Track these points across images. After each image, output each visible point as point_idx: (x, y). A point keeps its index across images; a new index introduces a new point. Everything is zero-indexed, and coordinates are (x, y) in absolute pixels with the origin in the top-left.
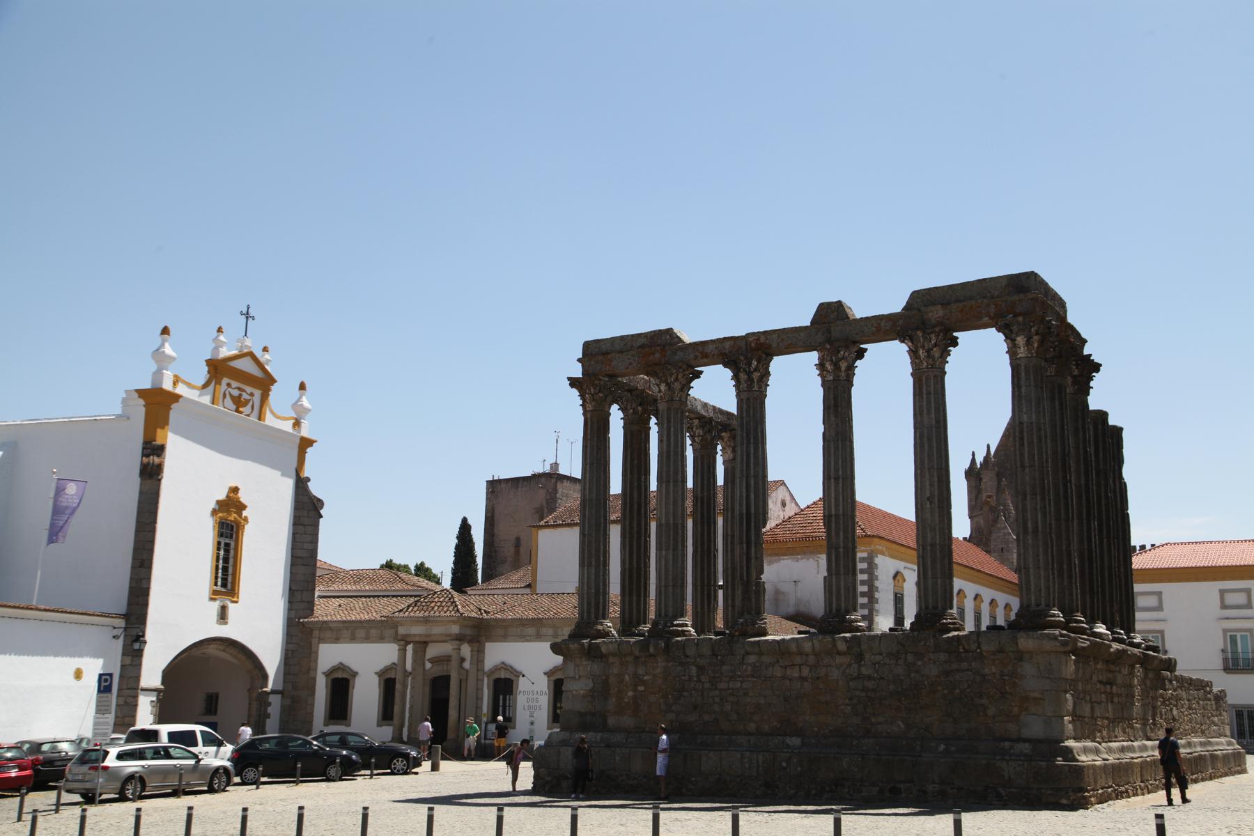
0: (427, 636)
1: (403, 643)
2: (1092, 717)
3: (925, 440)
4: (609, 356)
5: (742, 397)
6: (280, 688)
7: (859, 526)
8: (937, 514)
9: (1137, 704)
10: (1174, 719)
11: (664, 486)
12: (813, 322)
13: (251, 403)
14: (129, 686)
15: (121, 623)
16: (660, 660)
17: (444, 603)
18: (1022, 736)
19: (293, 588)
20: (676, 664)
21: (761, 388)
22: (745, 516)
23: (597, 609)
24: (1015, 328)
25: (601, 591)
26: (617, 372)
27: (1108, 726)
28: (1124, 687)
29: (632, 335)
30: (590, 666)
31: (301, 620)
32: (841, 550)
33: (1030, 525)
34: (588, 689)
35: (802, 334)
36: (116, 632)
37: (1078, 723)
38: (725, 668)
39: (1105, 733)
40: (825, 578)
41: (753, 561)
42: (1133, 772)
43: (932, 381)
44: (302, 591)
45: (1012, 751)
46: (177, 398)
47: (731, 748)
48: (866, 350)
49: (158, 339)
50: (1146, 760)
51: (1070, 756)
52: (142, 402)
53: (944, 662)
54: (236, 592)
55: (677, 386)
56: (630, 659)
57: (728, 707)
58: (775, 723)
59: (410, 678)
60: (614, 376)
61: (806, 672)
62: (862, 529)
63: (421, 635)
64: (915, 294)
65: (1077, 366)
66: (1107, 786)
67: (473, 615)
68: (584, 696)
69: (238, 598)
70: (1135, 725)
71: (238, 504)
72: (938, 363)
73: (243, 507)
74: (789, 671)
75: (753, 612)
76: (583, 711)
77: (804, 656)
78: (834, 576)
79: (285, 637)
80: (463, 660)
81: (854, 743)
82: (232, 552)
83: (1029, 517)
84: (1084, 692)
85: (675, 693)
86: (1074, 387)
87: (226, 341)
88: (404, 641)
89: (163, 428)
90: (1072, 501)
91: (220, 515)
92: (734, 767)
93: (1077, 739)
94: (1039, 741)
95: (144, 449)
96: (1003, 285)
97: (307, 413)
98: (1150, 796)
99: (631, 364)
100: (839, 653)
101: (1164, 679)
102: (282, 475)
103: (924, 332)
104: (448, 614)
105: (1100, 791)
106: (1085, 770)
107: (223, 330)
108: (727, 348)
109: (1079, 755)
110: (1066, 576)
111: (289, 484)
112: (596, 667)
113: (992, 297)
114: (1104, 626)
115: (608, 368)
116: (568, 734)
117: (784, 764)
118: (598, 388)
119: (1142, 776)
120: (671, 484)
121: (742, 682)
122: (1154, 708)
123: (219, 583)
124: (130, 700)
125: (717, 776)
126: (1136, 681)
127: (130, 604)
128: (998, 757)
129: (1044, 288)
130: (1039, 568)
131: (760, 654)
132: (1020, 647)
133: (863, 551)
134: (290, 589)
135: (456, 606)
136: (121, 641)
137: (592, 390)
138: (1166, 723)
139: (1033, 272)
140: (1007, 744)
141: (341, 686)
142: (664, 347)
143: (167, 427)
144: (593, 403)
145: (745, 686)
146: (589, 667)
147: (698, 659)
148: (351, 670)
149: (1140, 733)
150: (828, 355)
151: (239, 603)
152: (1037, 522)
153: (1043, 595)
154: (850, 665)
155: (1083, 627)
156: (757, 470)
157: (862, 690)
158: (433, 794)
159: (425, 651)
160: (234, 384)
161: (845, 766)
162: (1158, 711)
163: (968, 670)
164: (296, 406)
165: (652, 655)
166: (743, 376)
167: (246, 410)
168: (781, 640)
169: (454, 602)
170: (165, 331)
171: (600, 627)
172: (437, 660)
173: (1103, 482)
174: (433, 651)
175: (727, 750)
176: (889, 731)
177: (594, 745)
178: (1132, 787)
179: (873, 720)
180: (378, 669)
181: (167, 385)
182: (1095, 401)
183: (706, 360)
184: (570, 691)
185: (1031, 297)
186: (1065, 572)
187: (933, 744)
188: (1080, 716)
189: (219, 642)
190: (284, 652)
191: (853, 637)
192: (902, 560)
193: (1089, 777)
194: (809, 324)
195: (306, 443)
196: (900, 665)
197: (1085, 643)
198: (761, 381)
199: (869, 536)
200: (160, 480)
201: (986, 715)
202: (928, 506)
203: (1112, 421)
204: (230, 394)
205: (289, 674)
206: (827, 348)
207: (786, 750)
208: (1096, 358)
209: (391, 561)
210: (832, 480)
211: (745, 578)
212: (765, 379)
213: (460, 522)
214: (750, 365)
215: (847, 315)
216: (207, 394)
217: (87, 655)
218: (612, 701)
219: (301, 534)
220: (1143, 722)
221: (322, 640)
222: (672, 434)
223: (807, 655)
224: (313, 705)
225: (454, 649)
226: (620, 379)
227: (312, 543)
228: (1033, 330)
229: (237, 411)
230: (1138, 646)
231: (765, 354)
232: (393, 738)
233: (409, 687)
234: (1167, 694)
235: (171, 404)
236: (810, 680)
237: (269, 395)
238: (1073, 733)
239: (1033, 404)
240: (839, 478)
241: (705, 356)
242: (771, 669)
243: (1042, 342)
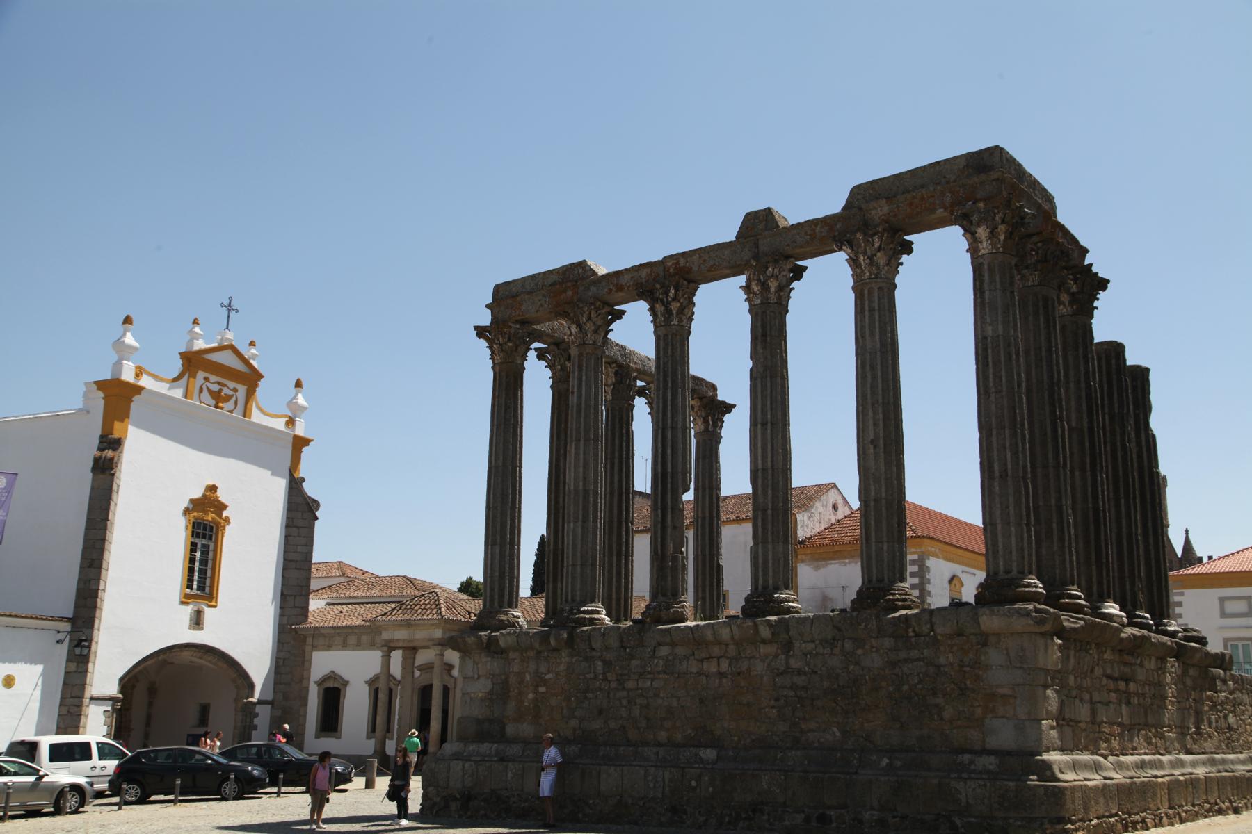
0: (410, 641)
1: (386, 649)
2: (1093, 722)
3: (868, 368)
4: (519, 299)
5: (659, 333)
6: (270, 697)
7: (910, 527)
8: (882, 461)
9: (1170, 707)
10: (1230, 728)
11: (573, 446)
12: (737, 237)
13: (234, 399)
14: (73, 695)
15: (67, 627)
16: (563, 654)
17: (429, 606)
18: (988, 746)
19: (285, 593)
20: (581, 659)
21: (682, 321)
22: (660, 475)
23: (501, 596)
24: (975, 218)
25: (507, 574)
26: (527, 316)
27: (1121, 735)
28: (1149, 685)
29: (544, 273)
30: (489, 664)
31: (293, 627)
32: (769, 512)
33: (996, 467)
34: (487, 690)
35: (726, 252)
36: (61, 636)
37: (1068, 730)
38: (634, 663)
39: (1115, 743)
40: (751, 547)
41: (669, 531)
42: (1154, 794)
43: (876, 295)
44: (295, 596)
45: (973, 767)
46: (138, 390)
47: (635, 763)
48: (806, 268)
49: (120, 328)
50: (1178, 780)
51: (1048, 773)
52: (101, 394)
53: (889, 650)
54: (215, 596)
55: (590, 327)
56: (531, 654)
57: (636, 711)
58: (689, 731)
59: (399, 687)
60: (528, 322)
61: (725, 666)
62: (913, 530)
63: (404, 640)
64: (855, 190)
65: (1075, 280)
66: (1107, 814)
67: (460, 618)
68: (482, 700)
69: (216, 602)
70: (1166, 734)
71: (216, 503)
72: (883, 272)
73: (224, 507)
74: (705, 665)
75: (669, 594)
76: (480, 717)
77: (723, 646)
78: (760, 545)
79: (276, 644)
80: (449, 667)
81: (779, 757)
82: (211, 554)
83: (996, 457)
84: (1080, 688)
85: (579, 695)
86: (1072, 307)
87: (201, 332)
88: (389, 648)
89: (122, 421)
90: (1064, 442)
91: (195, 514)
92: (636, 786)
93: (1062, 750)
94: (1009, 753)
95: (101, 442)
96: (961, 167)
97: (303, 412)
98: (1181, 827)
99: (541, 306)
100: (764, 642)
101: (1213, 678)
102: (272, 474)
103: (865, 234)
104: (430, 617)
105: (1095, 822)
106: (1068, 793)
107: (199, 322)
108: (643, 277)
109: (1063, 773)
110: (1055, 538)
111: (279, 487)
112: (495, 664)
113: (948, 182)
114: (1117, 606)
115: (517, 313)
116: (462, 745)
117: (694, 783)
118: (507, 336)
119: (1169, 800)
120: (582, 443)
121: (652, 680)
122: (1199, 716)
123: (195, 586)
124: (74, 710)
125: (618, 798)
126: (1168, 679)
127: (77, 606)
128: (953, 775)
129: (1015, 169)
130: (1009, 523)
131: (673, 644)
132: (983, 627)
133: (914, 553)
134: (282, 594)
135: (440, 608)
136: (65, 646)
137: (501, 339)
138: (1218, 733)
139: (997, 146)
140: (967, 757)
141: (332, 696)
142: (576, 282)
143: (126, 420)
144: (501, 354)
145: (655, 684)
146: (488, 664)
147: (605, 653)
148: (342, 679)
149: (1176, 745)
150: (754, 274)
151: (218, 607)
152: (1005, 464)
153: (1014, 558)
154: (776, 656)
155: (1079, 604)
156: (675, 420)
157: (791, 688)
158: (298, 817)
159: (414, 658)
160: (213, 378)
161: (765, 787)
162: (1205, 718)
163: (919, 659)
164: (292, 404)
165: (556, 650)
166: (660, 308)
167: (229, 405)
168: (695, 626)
169: (439, 604)
170: (128, 320)
171: (503, 617)
172: (427, 668)
173: (1118, 429)
174: (423, 657)
175: (631, 765)
176: (822, 740)
177: (486, 759)
178: (1152, 814)
179: (803, 727)
180: (368, 678)
181: (128, 375)
182: (1103, 329)
183: (621, 294)
184: (468, 693)
185: (995, 176)
186: (1055, 532)
187: (874, 757)
188: (1071, 720)
189: (194, 649)
190: (274, 659)
191: (780, 621)
192: (959, 563)
193: (1073, 802)
194: (734, 239)
195: (300, 443)
196: (835, 655)
197: (1077, 623)
198: (682, 313)
199: (919, 537)
200: (113, 475)
201: (942, 719)
202: (872, 451)
203: (1132, 359)
204: (208, 389)
205: (281, 684)
206: (752, 265)
207: (697, 765)
208: (1100, 269)
209: (471, 578)
210: (759, 426)
211: (659, 551)
212: (686, 311)
213: (538, 540)
214: (667, 293)
215: (777, 223)
216: (178, 387)
217: (21, 661)
218: (512, 705)
219: (294, 536)
220: (1179, 730)
221: (315, 647)
222: (584, 383)
223: (727, 645)
224: (305, 716)
225: (436, 655)
226: (535, 327)
227: (306, 545)
228: (997, 218)
229: (216, 406)
230: (1173, 635)
231: (685, 280)
232: (375, 752)
233: (399, 697)
234: (1218, 697)
235: (132, 397)
236: (730, 676)
237: (255, 391)
238: (1059, 743)
239: (1000, 311)
240: (766, 424)
241: (620, 288)
242: (685, 663)
243: (1011, 233)
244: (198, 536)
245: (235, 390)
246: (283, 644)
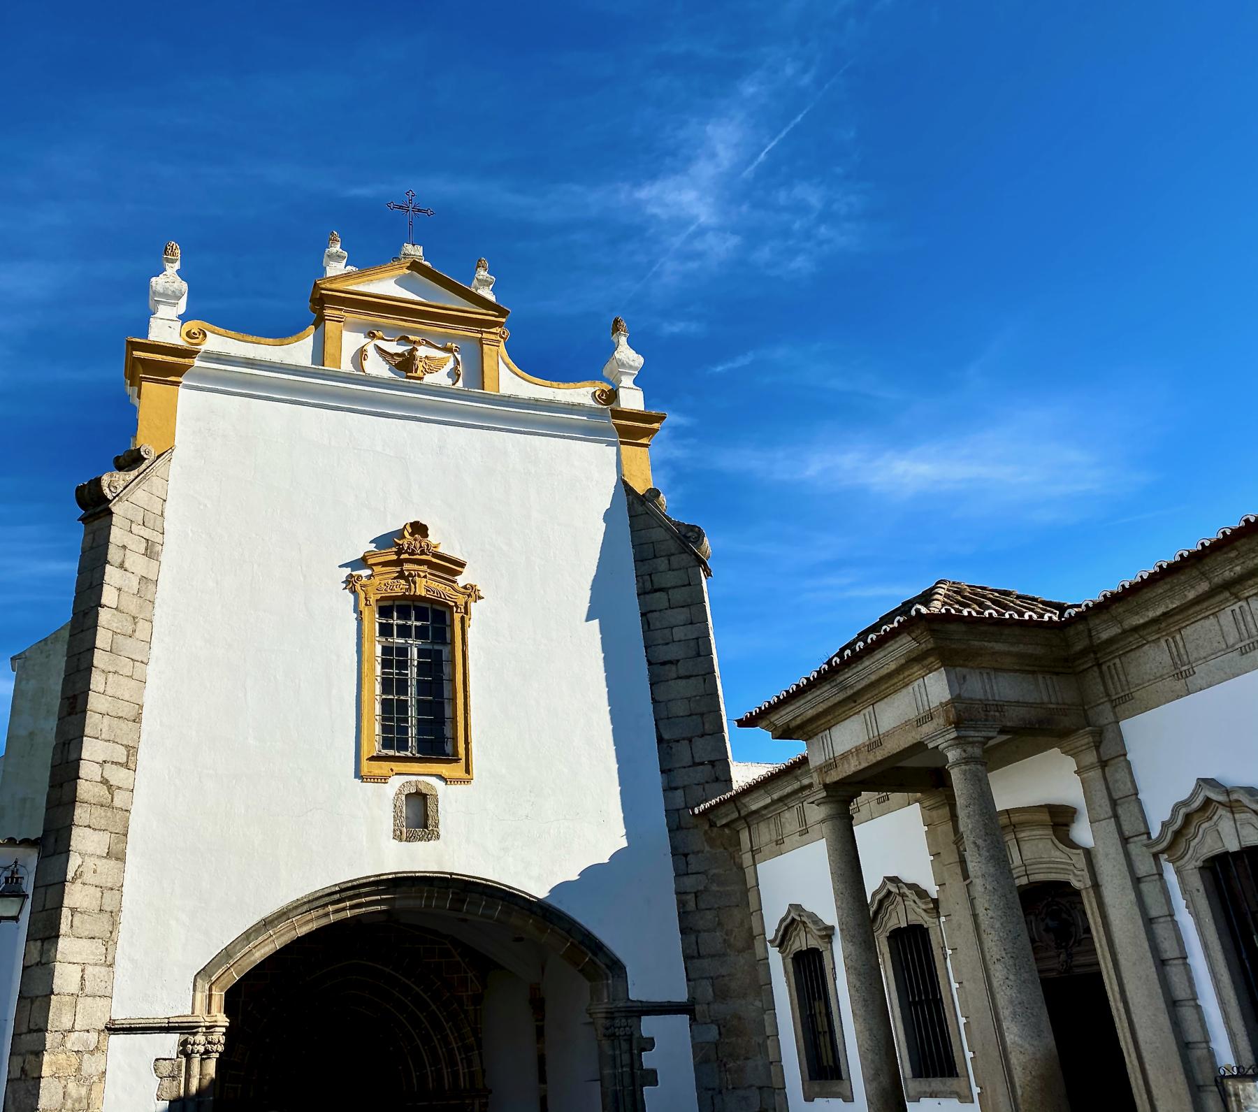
19: (666, 736)
31: (696, 811)
134: (660, 740)
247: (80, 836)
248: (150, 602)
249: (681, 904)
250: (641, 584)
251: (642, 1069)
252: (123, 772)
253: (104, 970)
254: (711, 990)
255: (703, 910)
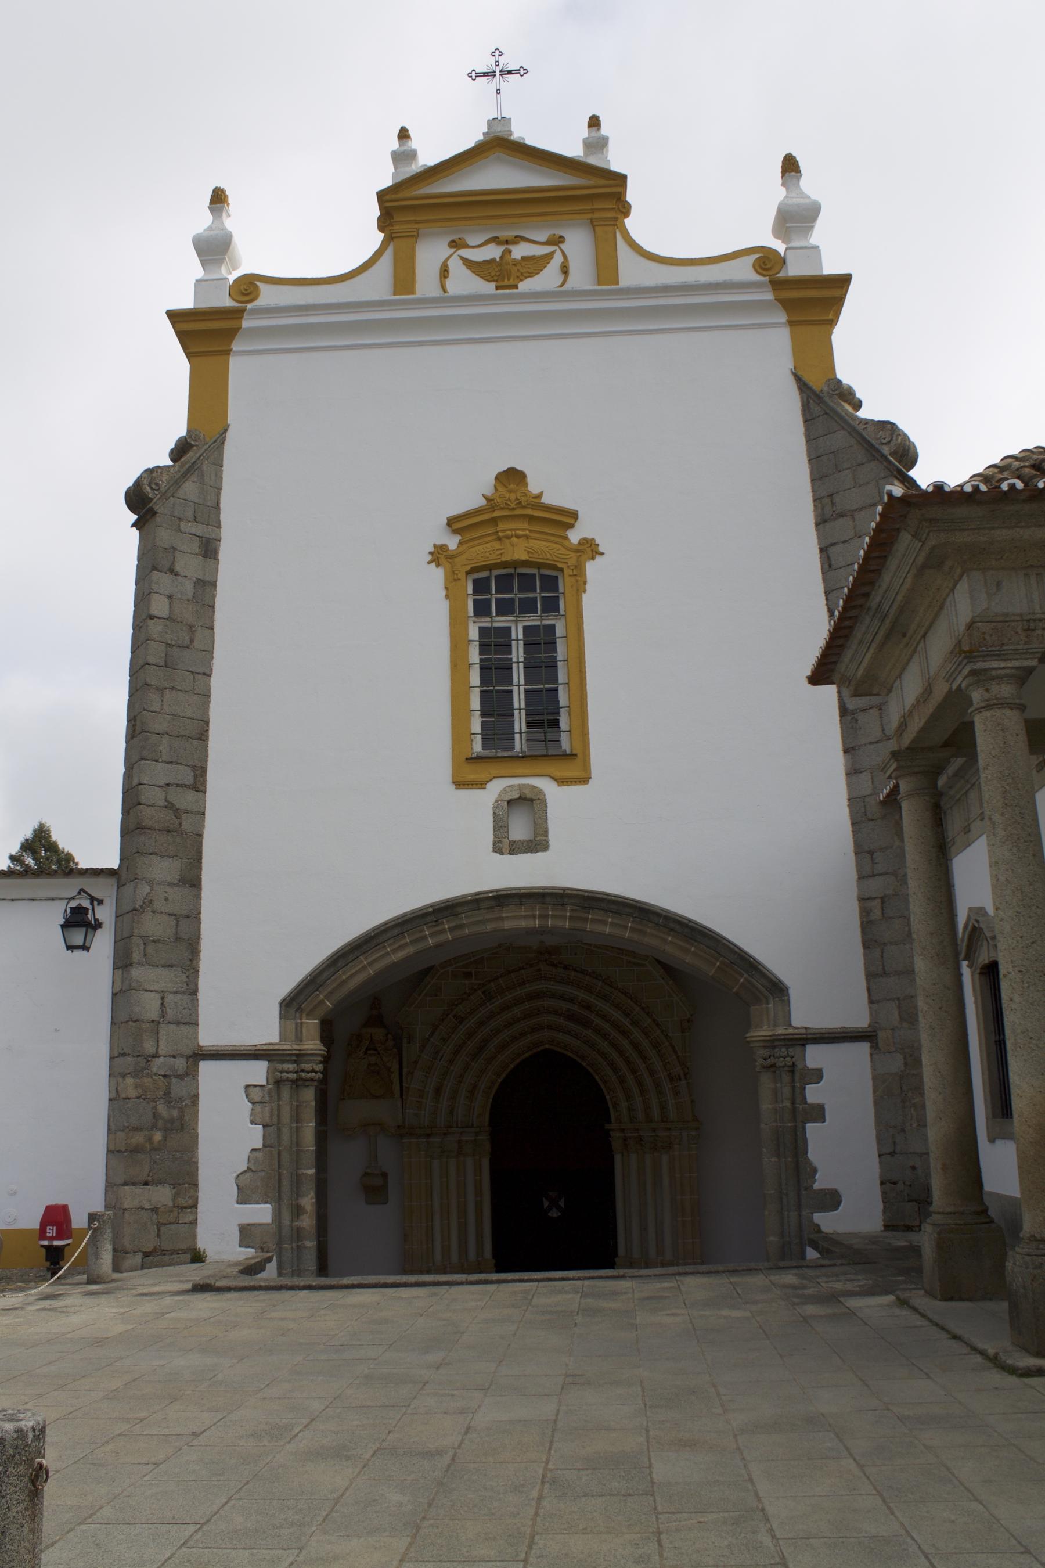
6: (861, 1020)
13: (558, 259)
204: (459, 256)
205: (885, 974)
244: (505, 608)
245: (561, 240)
246: (871, 853)
247: (145, 864)
248: (210, 606)
249: (865, 912)
250: (820, 510)
251: (806, 1103)
252: (191, 796)
253: (186, 997)
254: (896, 1013)
255: (890, 918)
